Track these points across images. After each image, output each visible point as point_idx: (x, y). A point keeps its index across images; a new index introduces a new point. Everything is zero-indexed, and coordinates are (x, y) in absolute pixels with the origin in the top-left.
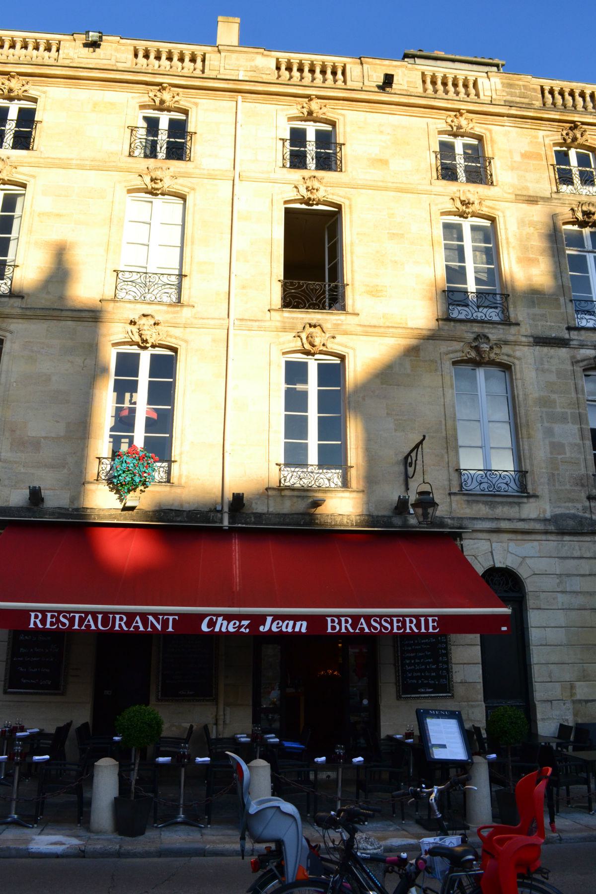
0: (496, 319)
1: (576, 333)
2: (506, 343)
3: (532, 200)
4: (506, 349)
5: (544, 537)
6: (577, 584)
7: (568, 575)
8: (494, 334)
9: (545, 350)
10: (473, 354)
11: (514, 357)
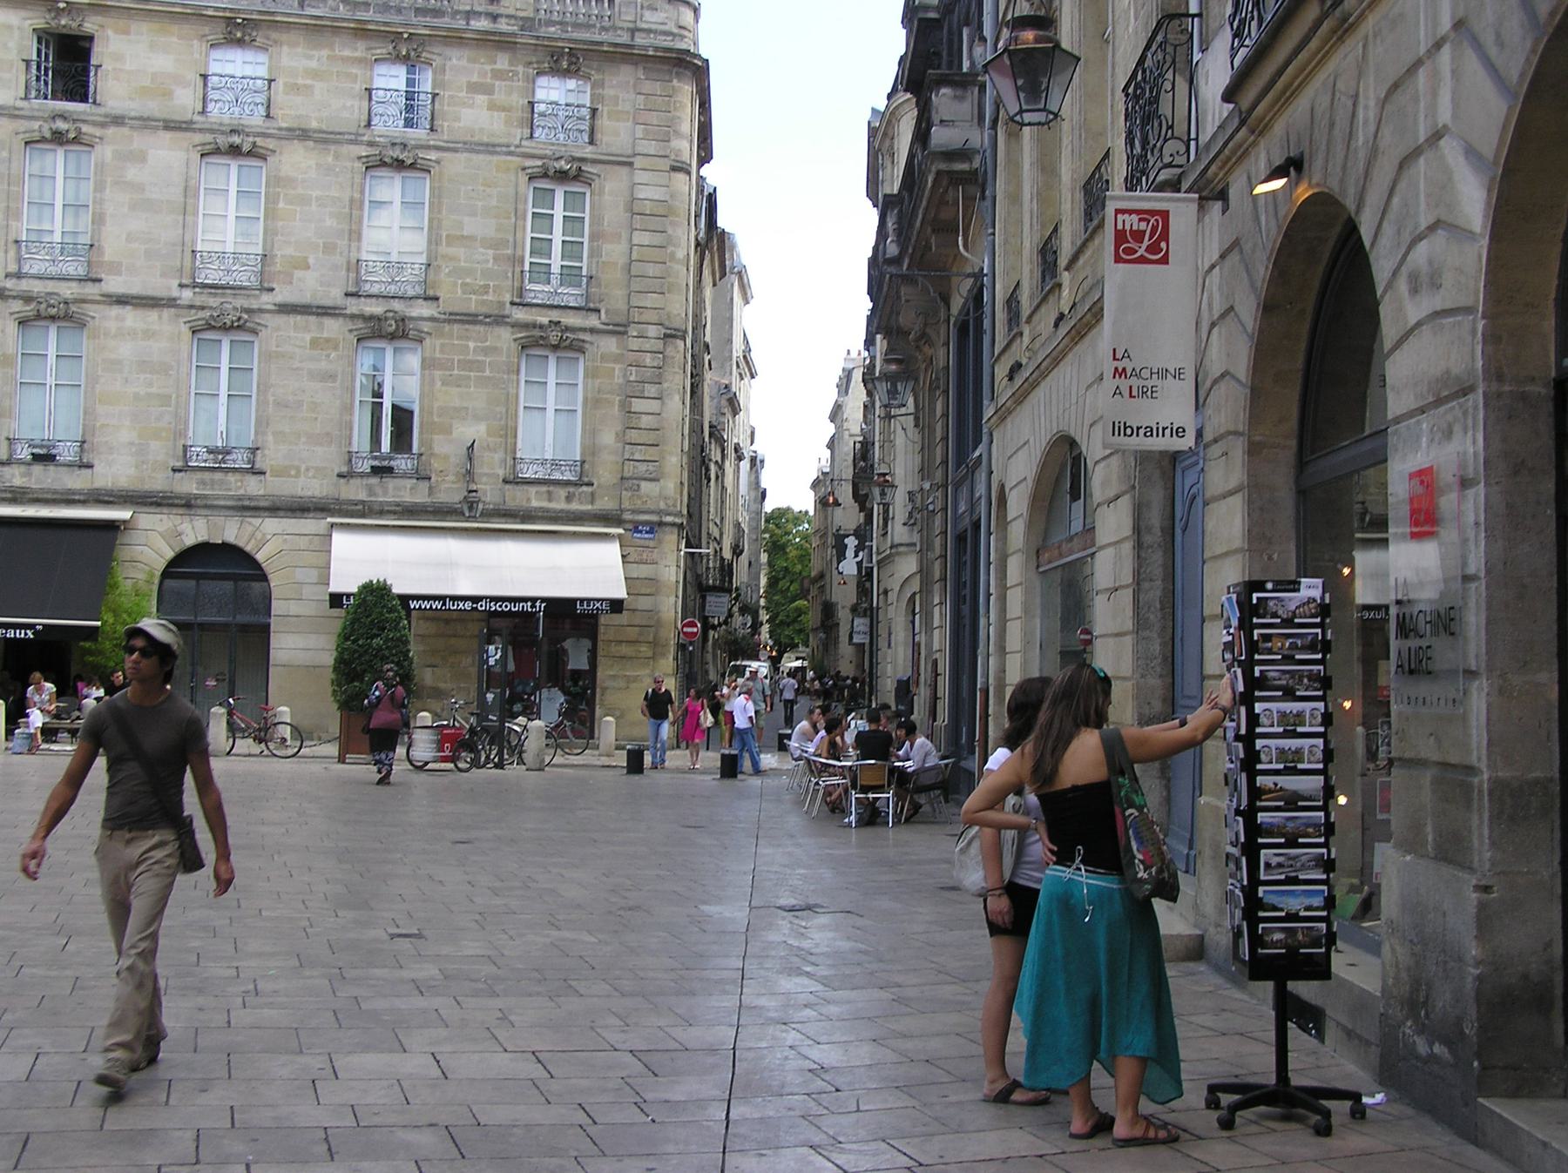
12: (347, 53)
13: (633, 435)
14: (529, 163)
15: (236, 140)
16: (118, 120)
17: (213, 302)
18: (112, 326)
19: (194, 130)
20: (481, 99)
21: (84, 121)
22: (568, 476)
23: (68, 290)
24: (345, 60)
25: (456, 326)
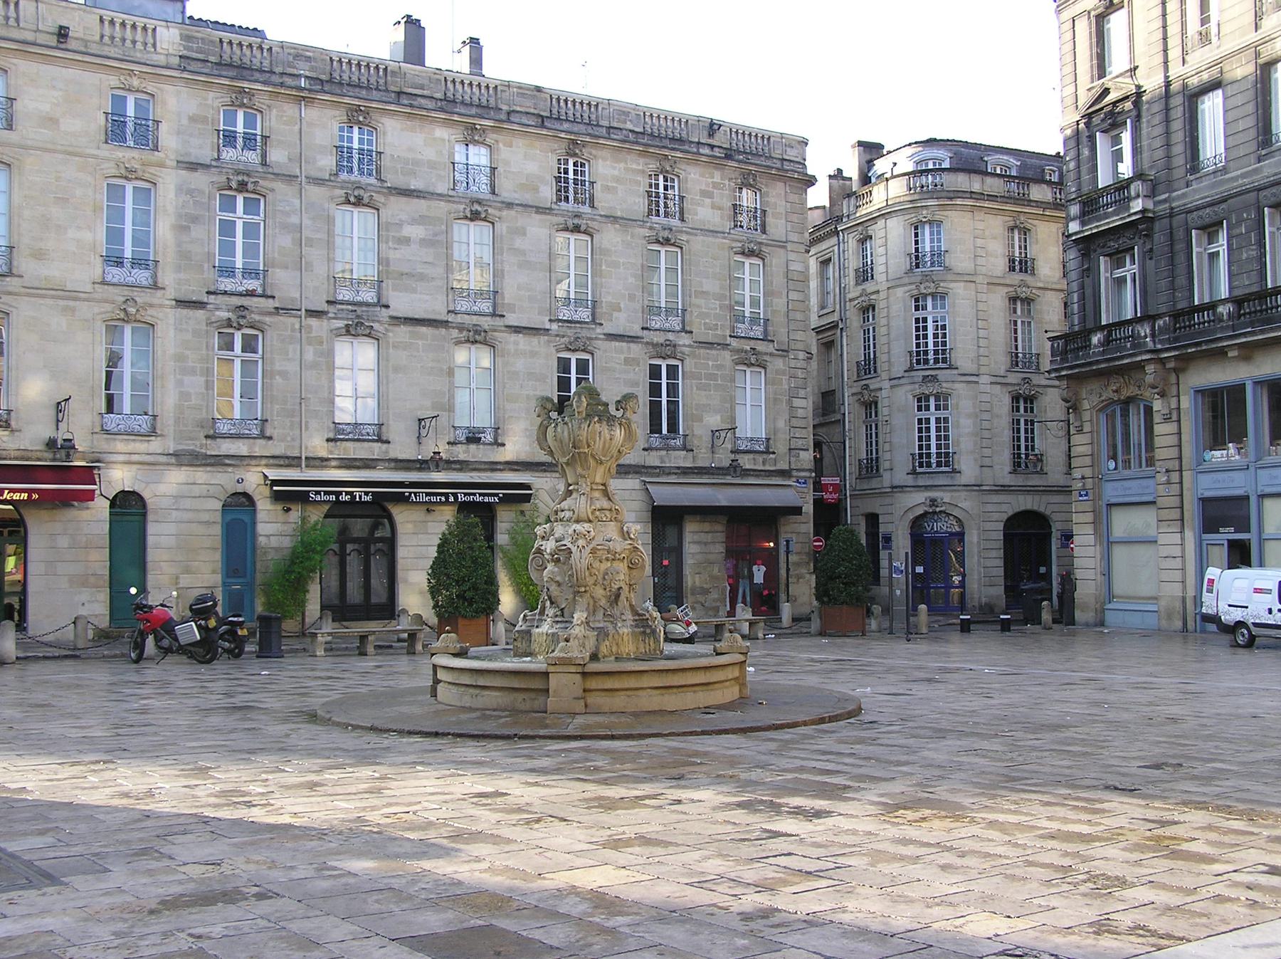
0: (145, 283)
2: (151, 306)
3: (193, 166)
4: (151, 311)
6: (187, 504)
9: (185, 311)
10: (122, 315)
15: (576, 221)
16: (510, 205)
17: (569, 332)
18: (512, 347)
20: (708, 201)
22: (762, 448)
24: (633, 171)
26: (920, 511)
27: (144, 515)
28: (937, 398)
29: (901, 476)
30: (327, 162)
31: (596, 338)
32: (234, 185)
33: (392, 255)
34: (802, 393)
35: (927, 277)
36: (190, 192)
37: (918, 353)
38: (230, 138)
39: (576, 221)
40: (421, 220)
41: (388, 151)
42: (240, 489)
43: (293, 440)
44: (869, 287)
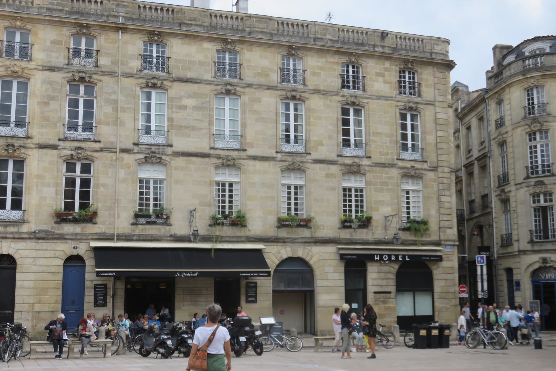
1: (62, 142)
2: (24, 147)
3: (52, 69)
4: (23, 151)
5: (29, 241)
6: (42, 262)
7: (38, 258)
8: (17, 143)
11: (27, 155)
12: (332, 60)
13: (443, 211)
14: (399, 104)
16: (250, 86)
17: (289, 159)
19: (278, 90)
20: (381, 79)
21: (238, 86)
23: (234, 154)
24: (332, 63)
25: (378, 168)
26: (536, 266)
27: (15, 269)
28: (545, 194)
29: (524, 245)
30: (136, 64)
31: (307, 162)
32: (77, 78)
33: (175, 116)
34: (447, 193)
35: (535, 120)
36: (50, 83)
37: (532, 167)
38: (77, 53)
39: (294, 93)
40: (195, 95)
41: (173, 56)
42: (75, 252)
43: (110, 224)
44: (503, 130)
